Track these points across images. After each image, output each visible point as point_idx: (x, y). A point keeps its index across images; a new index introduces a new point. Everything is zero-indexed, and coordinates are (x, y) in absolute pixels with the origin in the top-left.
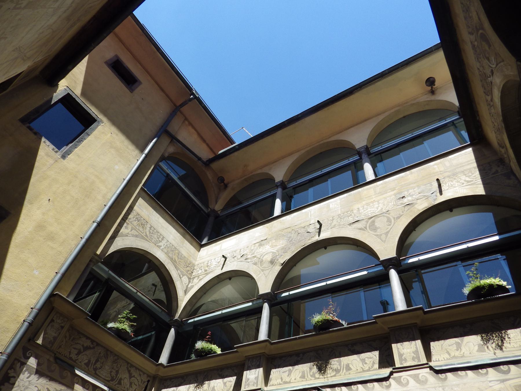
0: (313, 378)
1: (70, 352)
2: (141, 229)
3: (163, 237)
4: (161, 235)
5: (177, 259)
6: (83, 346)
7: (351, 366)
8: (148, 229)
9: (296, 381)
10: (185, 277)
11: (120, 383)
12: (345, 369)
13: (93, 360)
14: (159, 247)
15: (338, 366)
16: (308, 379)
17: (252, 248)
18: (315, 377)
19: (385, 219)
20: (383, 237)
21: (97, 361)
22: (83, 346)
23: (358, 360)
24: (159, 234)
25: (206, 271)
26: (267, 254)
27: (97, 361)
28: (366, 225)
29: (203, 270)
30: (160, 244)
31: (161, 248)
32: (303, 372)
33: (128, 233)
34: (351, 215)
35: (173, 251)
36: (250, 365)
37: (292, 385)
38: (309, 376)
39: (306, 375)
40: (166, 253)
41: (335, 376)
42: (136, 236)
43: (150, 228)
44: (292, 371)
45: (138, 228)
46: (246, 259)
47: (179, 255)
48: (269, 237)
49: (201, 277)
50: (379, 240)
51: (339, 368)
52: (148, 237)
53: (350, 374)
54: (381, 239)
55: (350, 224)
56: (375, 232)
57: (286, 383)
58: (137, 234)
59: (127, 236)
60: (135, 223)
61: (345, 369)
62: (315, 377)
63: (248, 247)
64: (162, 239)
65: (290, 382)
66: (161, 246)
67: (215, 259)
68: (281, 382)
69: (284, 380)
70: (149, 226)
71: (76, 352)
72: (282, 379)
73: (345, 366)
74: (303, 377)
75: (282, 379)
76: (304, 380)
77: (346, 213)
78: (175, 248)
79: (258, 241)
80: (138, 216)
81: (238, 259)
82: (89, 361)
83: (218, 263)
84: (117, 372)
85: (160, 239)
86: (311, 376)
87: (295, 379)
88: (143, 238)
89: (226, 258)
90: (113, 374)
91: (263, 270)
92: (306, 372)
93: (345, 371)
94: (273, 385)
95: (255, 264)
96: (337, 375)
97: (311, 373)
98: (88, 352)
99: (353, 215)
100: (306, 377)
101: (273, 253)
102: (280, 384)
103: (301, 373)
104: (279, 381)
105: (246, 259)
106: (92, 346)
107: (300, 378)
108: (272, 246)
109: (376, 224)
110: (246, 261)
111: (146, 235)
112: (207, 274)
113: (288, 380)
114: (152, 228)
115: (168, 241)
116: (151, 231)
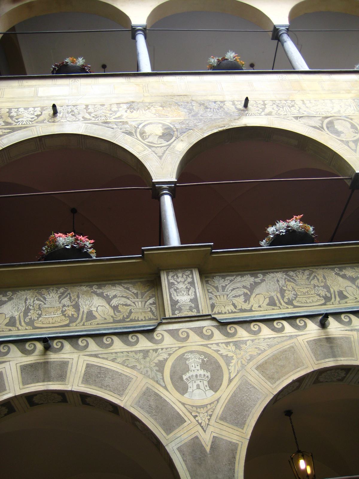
0: (290, 307)
7: (345, 293)
9: (261, 309)
12: (337, 296)
15: (327, 293)
16: (281, 307)
18: (292, 304)
19: (349, 126)
20: (352, 145)
23: (355, 287)
28: (322, 124)
34: (293, 106)
36: (171, 281)
38: (283, 304)
39: (277, 302)
41: (324, 304)
44: (250, 297)
46: (106, 123)
48: (148, 100)
50: (346, 147)
51: (328, 295)
53: (346, 303)
54: (348, 146)
55: (296, 118)
56: (339, 136)
57: (242, 311)
61: (337, 296)
62: (292, 304)
65: (251, 310)
68: (234, 310)
69: (239, 307)
73: (336, 293)
74: (272, 303)
76: (275, 308)
77: (284, 102)
83: (38, 116)
86: (286, 303)
87: (260, 307)
91: (150, 147)
92: (276, 298)
93: (338, 299)
94: (219, 313)
95: (130, 134)
96: (328, 303)
97: (286, 301)
99: (295, 105)
100: (278, 304)
101: (164, 125)
102: (232, 312)
103: (268, 299)
104: (231, 308)
107: (268, 305)
109: (336, 127)
110: (107, 125)
113: (246, 306)
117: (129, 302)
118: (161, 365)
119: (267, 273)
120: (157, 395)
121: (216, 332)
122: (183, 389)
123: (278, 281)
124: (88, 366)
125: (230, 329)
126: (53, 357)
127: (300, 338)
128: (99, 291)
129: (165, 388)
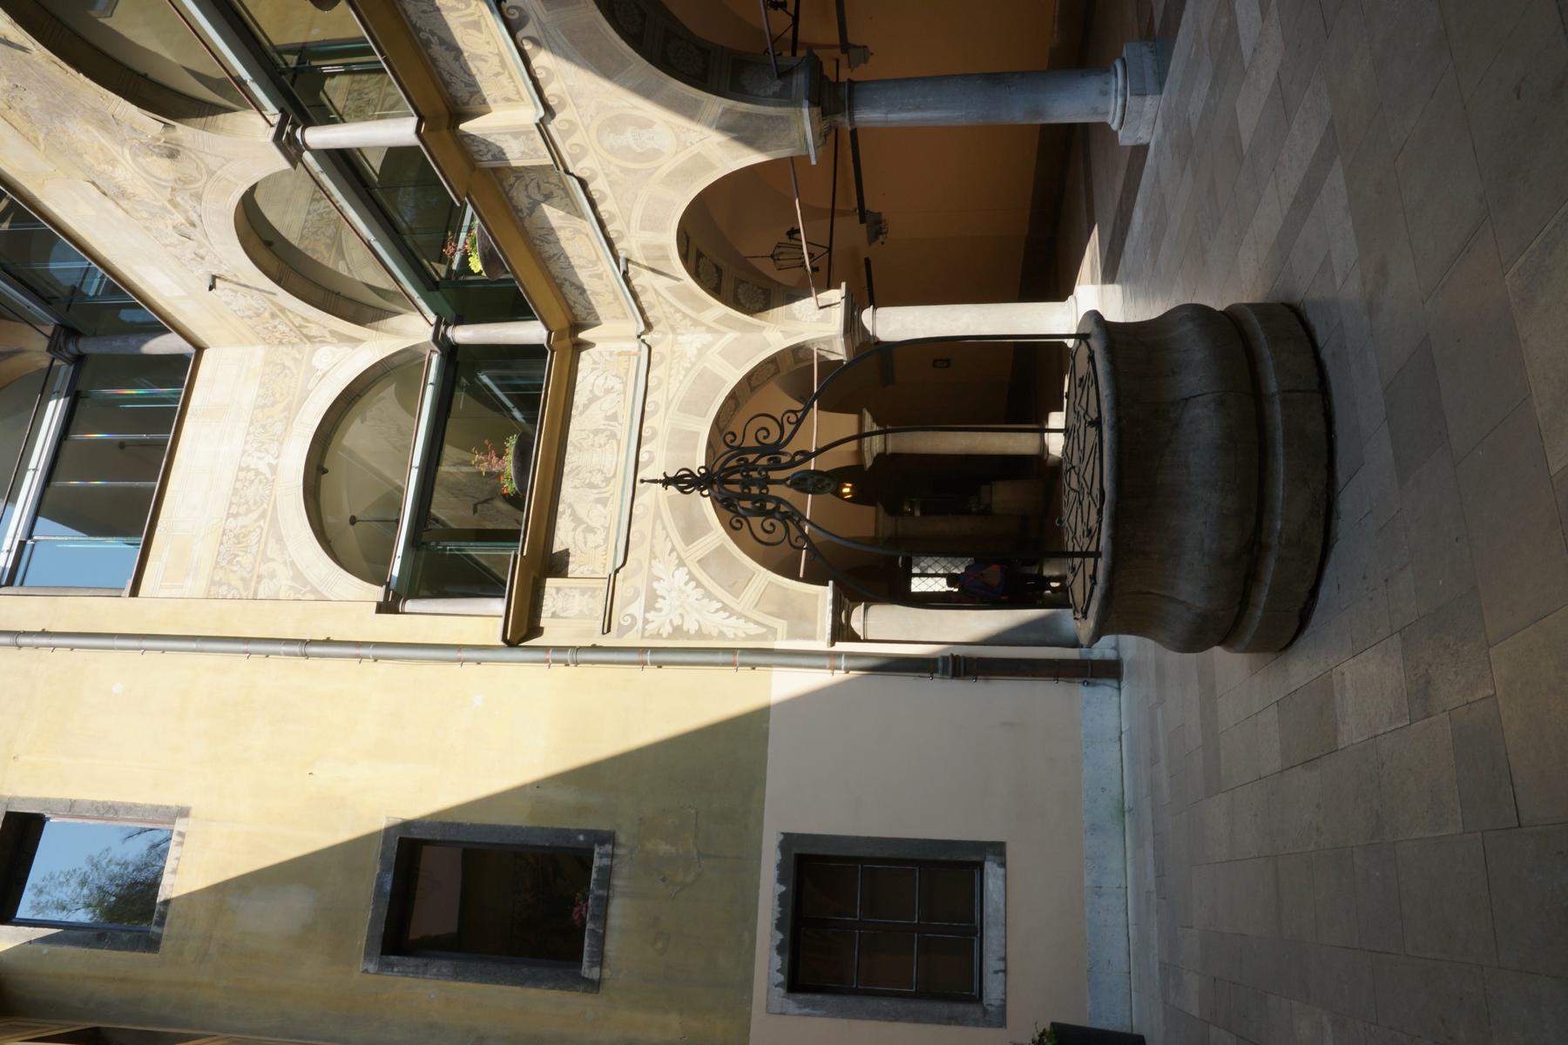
1: (596, 547)
2: (253, 538)
3: (241, 469)
4: (237, 480)
5: (280, 406)
6: (574, 529)
8: (241, 521)
10: (315, 362)
11: (614, 417)
13: (593, 494)
14: (273, 469)
17: (145, 215)
21: (591, 486)
22: (574, 529)
24: (239, 485)
25: (273, 316)
26: (146, 172)
27: (591, 486)
29: (276, 322)
30: (264, 469)
31: (274, 462)
32: (466, 25)
33: (285, 563)
35: (263, 426)
37: (504, 49)
40: (281, 444)
42: (280, 540)
43: (235, 516)
45: (255, 549)
46: (194, 225)
47: (265, 406)
49: (298, 321)
52: (265, 511)
57: (503, 64)
58: (272, 542)
59: (292, 563)
60: (246, 560)
63: (147, 228)
64: (248, 469)
65: (499, 55)
66: (270, 465)
67: (228, 304)
70: (232, 523)
71: (590, 537)
72: (497, 74)
75: (497, 74)
78: (251, 423)
79: (110, 205)
80: (224, 563)
81: (201, 246)
82: (597, 501)
84: (596, 432)
85: (251, 475)
88: (274, 520)
89: (214, 278)
90: (601, 439)
98: (582, 513)
100: (475, 18)
104: (504, 79)
105: (194, 225)
106: (568, 512)
107: (480, 31)
108: (113, 162)
110: (197, 221)
111: (263, 516)
112: (282, 310)
113: (495, 61)
114: (234, 510)
115: (244, 452)
116: (242, 510)
117: (533, 184)
118: (625, 171)
119: (414, 26)
120: (668, 175)
121: (559, 116)
122: (656, 153)
123: (424, 12)
124: (642, 228)
125: (553, 102)
126: (638, 256)
127: (543, 18)
128: (526, 212)
129: (657, 168)
